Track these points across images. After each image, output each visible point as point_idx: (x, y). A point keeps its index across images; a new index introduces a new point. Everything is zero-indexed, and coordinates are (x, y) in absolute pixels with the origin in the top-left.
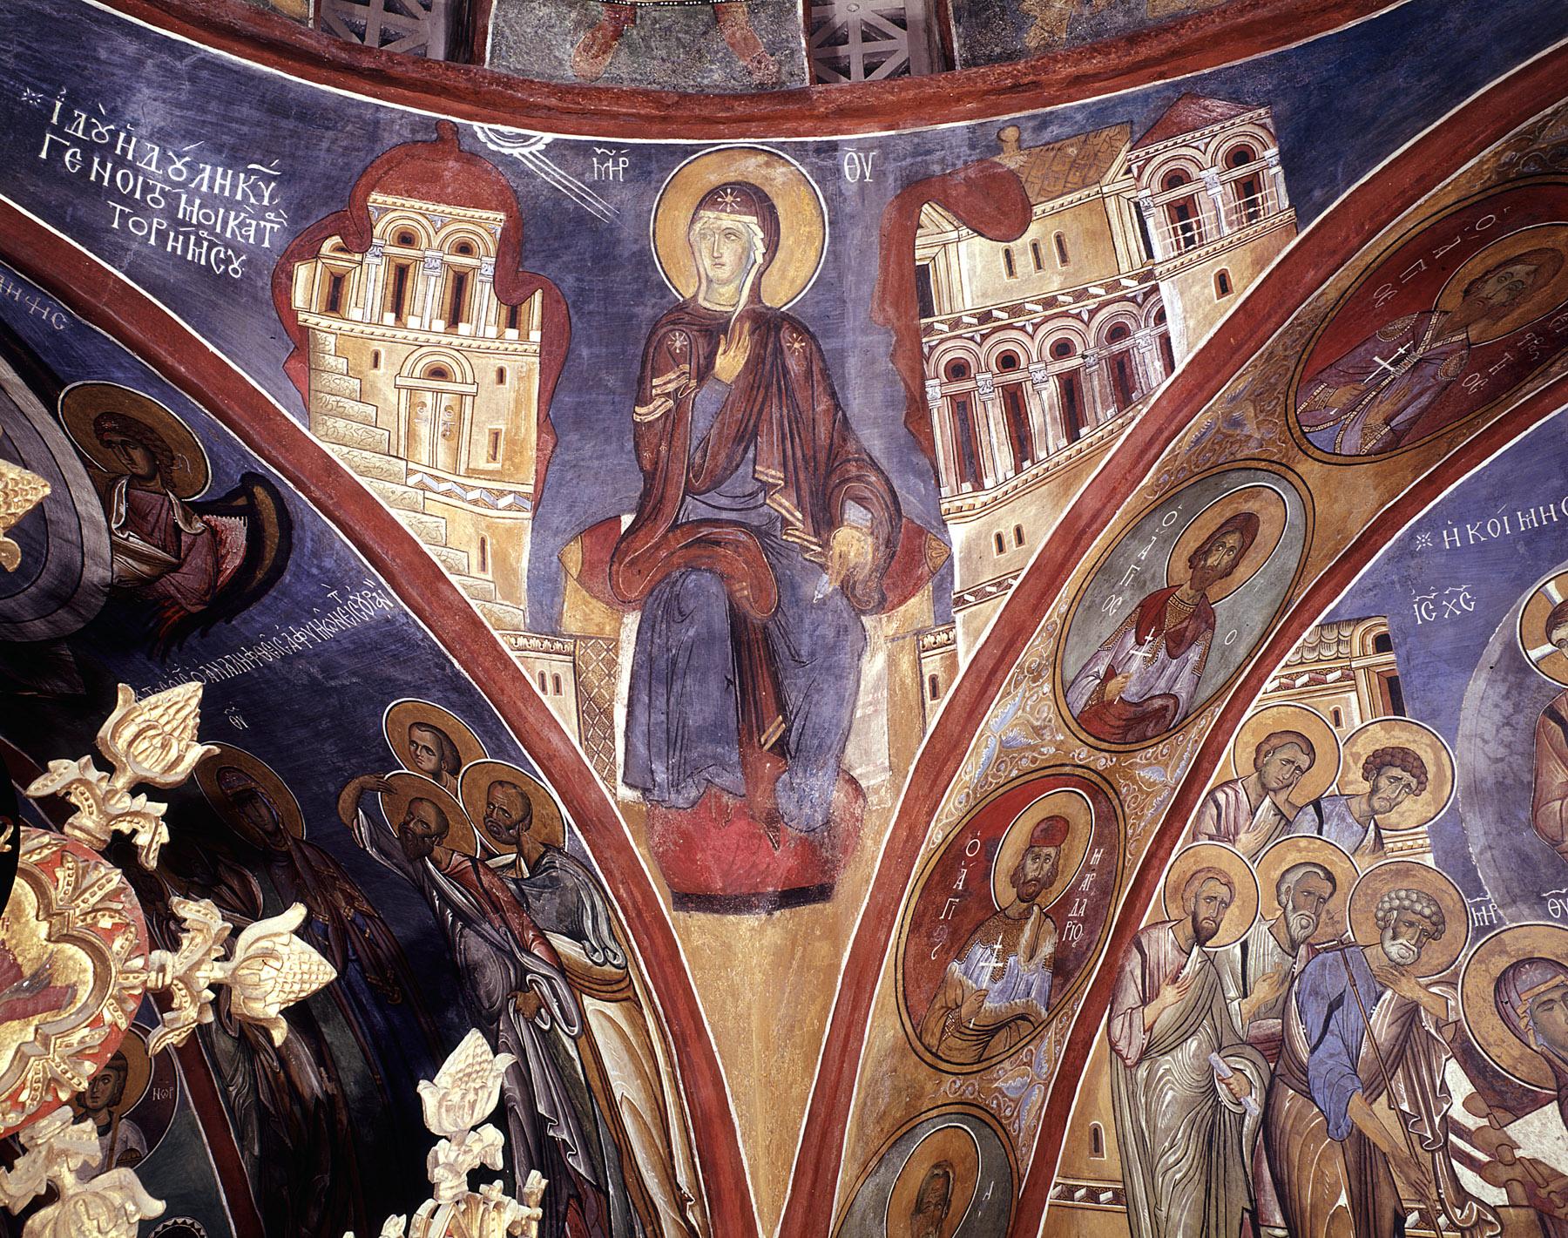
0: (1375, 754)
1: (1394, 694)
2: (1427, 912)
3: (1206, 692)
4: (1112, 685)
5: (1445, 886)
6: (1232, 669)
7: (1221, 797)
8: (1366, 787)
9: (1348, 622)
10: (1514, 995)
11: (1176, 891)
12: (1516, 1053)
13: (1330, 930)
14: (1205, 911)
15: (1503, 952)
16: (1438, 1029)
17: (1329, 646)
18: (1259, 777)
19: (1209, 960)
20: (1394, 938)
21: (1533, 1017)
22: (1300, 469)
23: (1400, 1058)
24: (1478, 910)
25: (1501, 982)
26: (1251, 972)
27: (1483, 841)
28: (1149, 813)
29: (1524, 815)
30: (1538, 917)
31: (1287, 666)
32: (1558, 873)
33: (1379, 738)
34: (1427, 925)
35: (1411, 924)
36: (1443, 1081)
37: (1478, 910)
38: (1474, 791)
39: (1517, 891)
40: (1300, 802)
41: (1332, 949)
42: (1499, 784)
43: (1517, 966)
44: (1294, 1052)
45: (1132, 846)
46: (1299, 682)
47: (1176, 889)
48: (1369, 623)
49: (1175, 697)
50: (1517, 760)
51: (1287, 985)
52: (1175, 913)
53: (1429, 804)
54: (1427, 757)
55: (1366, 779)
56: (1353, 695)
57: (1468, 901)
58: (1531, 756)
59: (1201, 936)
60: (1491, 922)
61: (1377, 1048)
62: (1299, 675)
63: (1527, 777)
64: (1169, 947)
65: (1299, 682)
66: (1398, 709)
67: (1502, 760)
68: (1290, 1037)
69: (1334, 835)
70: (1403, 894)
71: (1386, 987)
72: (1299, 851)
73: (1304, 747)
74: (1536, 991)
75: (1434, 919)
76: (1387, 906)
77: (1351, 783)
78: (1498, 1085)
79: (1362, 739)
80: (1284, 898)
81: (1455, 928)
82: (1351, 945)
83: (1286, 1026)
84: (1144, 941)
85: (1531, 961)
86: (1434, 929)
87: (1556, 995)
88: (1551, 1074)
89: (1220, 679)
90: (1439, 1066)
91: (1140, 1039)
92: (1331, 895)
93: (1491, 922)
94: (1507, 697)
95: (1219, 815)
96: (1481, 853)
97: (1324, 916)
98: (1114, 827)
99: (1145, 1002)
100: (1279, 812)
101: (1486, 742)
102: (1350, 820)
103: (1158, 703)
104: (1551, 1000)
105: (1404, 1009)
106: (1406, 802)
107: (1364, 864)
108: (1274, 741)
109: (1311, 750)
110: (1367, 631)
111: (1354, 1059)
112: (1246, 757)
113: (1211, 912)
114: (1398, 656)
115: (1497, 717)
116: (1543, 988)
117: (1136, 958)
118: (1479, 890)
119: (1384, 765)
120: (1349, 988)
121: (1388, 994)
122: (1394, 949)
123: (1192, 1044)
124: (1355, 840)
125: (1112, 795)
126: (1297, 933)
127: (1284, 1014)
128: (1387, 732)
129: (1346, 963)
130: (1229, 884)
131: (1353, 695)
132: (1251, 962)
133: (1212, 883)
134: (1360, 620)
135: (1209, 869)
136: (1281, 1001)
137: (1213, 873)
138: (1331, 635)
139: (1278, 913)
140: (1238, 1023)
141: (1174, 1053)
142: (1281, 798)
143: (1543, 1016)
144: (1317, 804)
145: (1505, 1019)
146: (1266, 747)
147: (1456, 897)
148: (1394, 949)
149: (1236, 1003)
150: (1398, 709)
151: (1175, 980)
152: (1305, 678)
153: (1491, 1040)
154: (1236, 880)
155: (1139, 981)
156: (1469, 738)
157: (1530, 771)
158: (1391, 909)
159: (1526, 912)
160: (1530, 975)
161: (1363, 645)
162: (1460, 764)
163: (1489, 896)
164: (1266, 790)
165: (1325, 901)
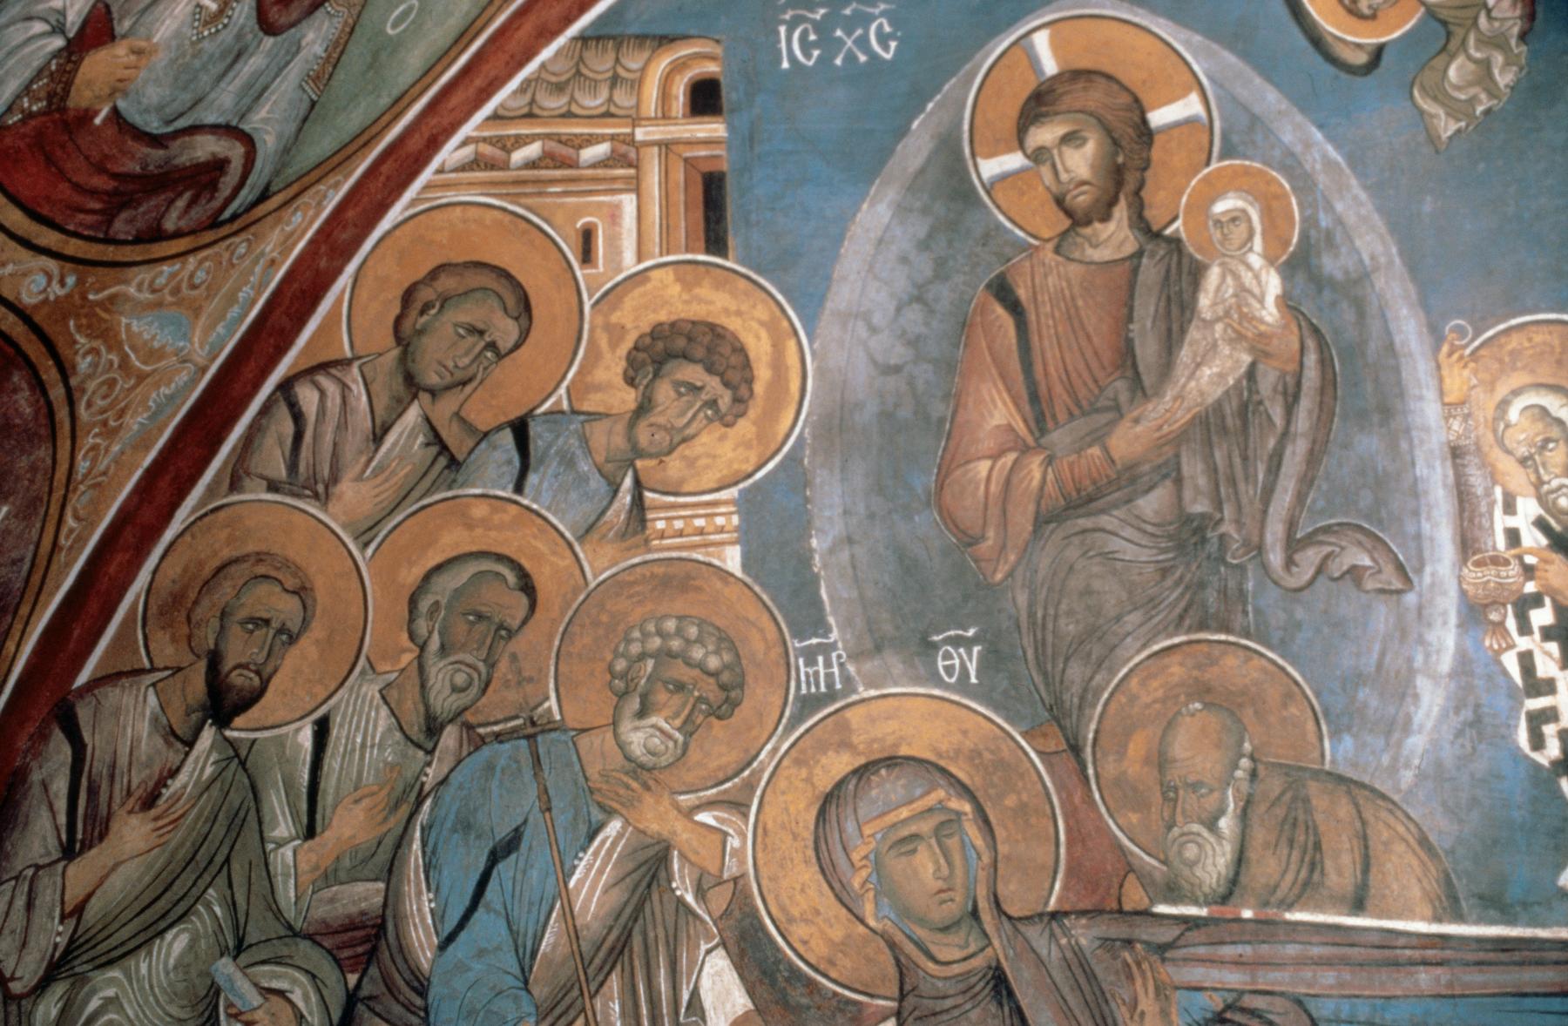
0: (657, 332)
1: (712, 207)
2: (713, 663)
3: (321, 144)
4: (98, 66)
5: (753, 612)
6: (385, 101)
7: (307, 397)
8: (628, 398)
9: (641, 39)
10: (850, 826)
11: (173, 607)
12: (837, 934)
13: (513, 696)
14: (240, 650)
15: (846, 745)
16: (700, 893)
17: (594, 86)
18: (404, 359)
19: (238, 757)
20: (642, 713)
21: (878, 866)
23: (620, 950)
24: (811, 662)
25: (830, 802)
26: (329, 784)
27: (838, 529)
28: (135, 422)
29: (923, 481)
30: (917, 681)
31: (495, 117)
32: (966, 598)
33: (671, 300)
34: (710, 689)
35: (680, 687)
36: (695, 994)
37: (811, 662)
38: (835, 428)
39: (888, 628)
40: (483, 421)
41: (512, 734)
42: (886, 416)
43: (862, 772)
44: (402, 950)
45: (80, 500)
46: (518, 156)
47: (177, 598)
48: (684, 50)
49: (248, 140)
50: (924, 373)
51: (405, 810)
52: (167, 651)
53: (748, 445)
54: (759, 347)
55: (631, 381)
56: (628, 202)
57: (795, 644)
58: (948, 367)
59: (223, 704)
60: (830, 685)
61: (575, 934)
62: (520, 141)
63: (938, 409)
64: (145, 728)
65: (518, 156)
66: (715, 241)
67: (897, 369)
68: (399, 918)
69: (546, 497)
70: (671, 625)
71: (610, 813)
72: (470, 526)
73: (511, 301)
74: (891, 818)
75: (726, 677)
76: (635, 649)
77: (598, 388)
78: (798, 996)
79: (631, 300)
80: (422, 626)
81: (760, 696)
82: (551, 727)
83: (392, 899)
84: (84, 713)
85: (892, 761)
86: (726, 697)
87: (925, 827)
88: (892, 971)
89: (354, 120)
90: (692, 962)
91: (52, 934)
92: (524, 622)
93: (830, 685)
94: (924, 245)
95: (298, 437)
96: (832, 551)
97: (503, 666)
98: (43, 452)
99: (70, 851)
100: (436, 439)
101: (873, 330)
102: (584, 466)
103: (206, 147)
104: (915, 837)
105: (642, 856)
106: (704, 438)
107: (600, 564)
108: (447, 283)
109: (524, 308)
110: (678, 67)
111: (526, 957)
112: (382, 308)
113: (255, 653)
114: (731, 128)
115: (901, 284)
116: (904, 813)
117: (60, 751)
118: (821, 627)
119: (670, 355)
120: (536, 817)
121: (614, 827)
122: (638, 738)
123: (176, 943)
124: (588, 510)
125: (50, 374)
126: (443, 700)
127: (391, 871)
128: (687, 286)
129: (537, 761)
130: (302, 592)
131: (628, 202)
132: (332, 763)
133: (263, 589)
134: (665, 40)
135: (260, 557)
136: (389, 842)
137: (264, 566)
138: (600, 63)
139: (407, 658)
140: (287, 893)
141: (131, 962)
142: (443, 410)
143: (897, 865)
144: (520, 430)
145: (827, 870)
146: (425, 294)
147: (771, 633)
148: (638, 738)
149: (287, 852)
150: (715, 241)
151: (150, 801)
152: (533, 150)
153: (795, 912)
154: (320, 585)
155: (61, 805)
156: (845, 318)
157: (946, 397)
158: (642, 657)
159: (897, 667)
160: (888, 788)
161: (665, 96)
162: (820, 372)
163: (834, 635)
164: (412, 385)
165: (511, 634)
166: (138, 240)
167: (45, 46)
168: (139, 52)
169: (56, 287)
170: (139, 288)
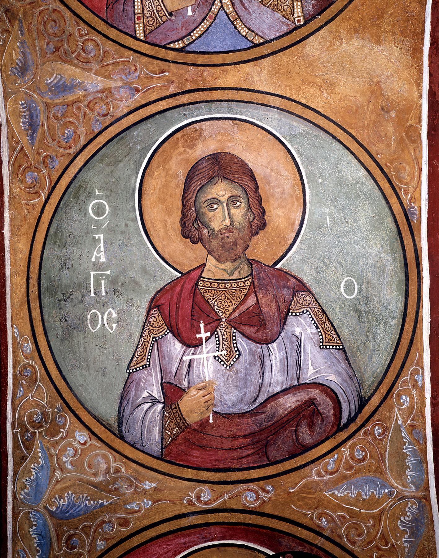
6: (395, 323)
22: (222, 82)
103: (290, 402)
166: (292, 456)
167: (154, 412)
168: (204, 388)
169: (262, 495)
170: (319, 474)
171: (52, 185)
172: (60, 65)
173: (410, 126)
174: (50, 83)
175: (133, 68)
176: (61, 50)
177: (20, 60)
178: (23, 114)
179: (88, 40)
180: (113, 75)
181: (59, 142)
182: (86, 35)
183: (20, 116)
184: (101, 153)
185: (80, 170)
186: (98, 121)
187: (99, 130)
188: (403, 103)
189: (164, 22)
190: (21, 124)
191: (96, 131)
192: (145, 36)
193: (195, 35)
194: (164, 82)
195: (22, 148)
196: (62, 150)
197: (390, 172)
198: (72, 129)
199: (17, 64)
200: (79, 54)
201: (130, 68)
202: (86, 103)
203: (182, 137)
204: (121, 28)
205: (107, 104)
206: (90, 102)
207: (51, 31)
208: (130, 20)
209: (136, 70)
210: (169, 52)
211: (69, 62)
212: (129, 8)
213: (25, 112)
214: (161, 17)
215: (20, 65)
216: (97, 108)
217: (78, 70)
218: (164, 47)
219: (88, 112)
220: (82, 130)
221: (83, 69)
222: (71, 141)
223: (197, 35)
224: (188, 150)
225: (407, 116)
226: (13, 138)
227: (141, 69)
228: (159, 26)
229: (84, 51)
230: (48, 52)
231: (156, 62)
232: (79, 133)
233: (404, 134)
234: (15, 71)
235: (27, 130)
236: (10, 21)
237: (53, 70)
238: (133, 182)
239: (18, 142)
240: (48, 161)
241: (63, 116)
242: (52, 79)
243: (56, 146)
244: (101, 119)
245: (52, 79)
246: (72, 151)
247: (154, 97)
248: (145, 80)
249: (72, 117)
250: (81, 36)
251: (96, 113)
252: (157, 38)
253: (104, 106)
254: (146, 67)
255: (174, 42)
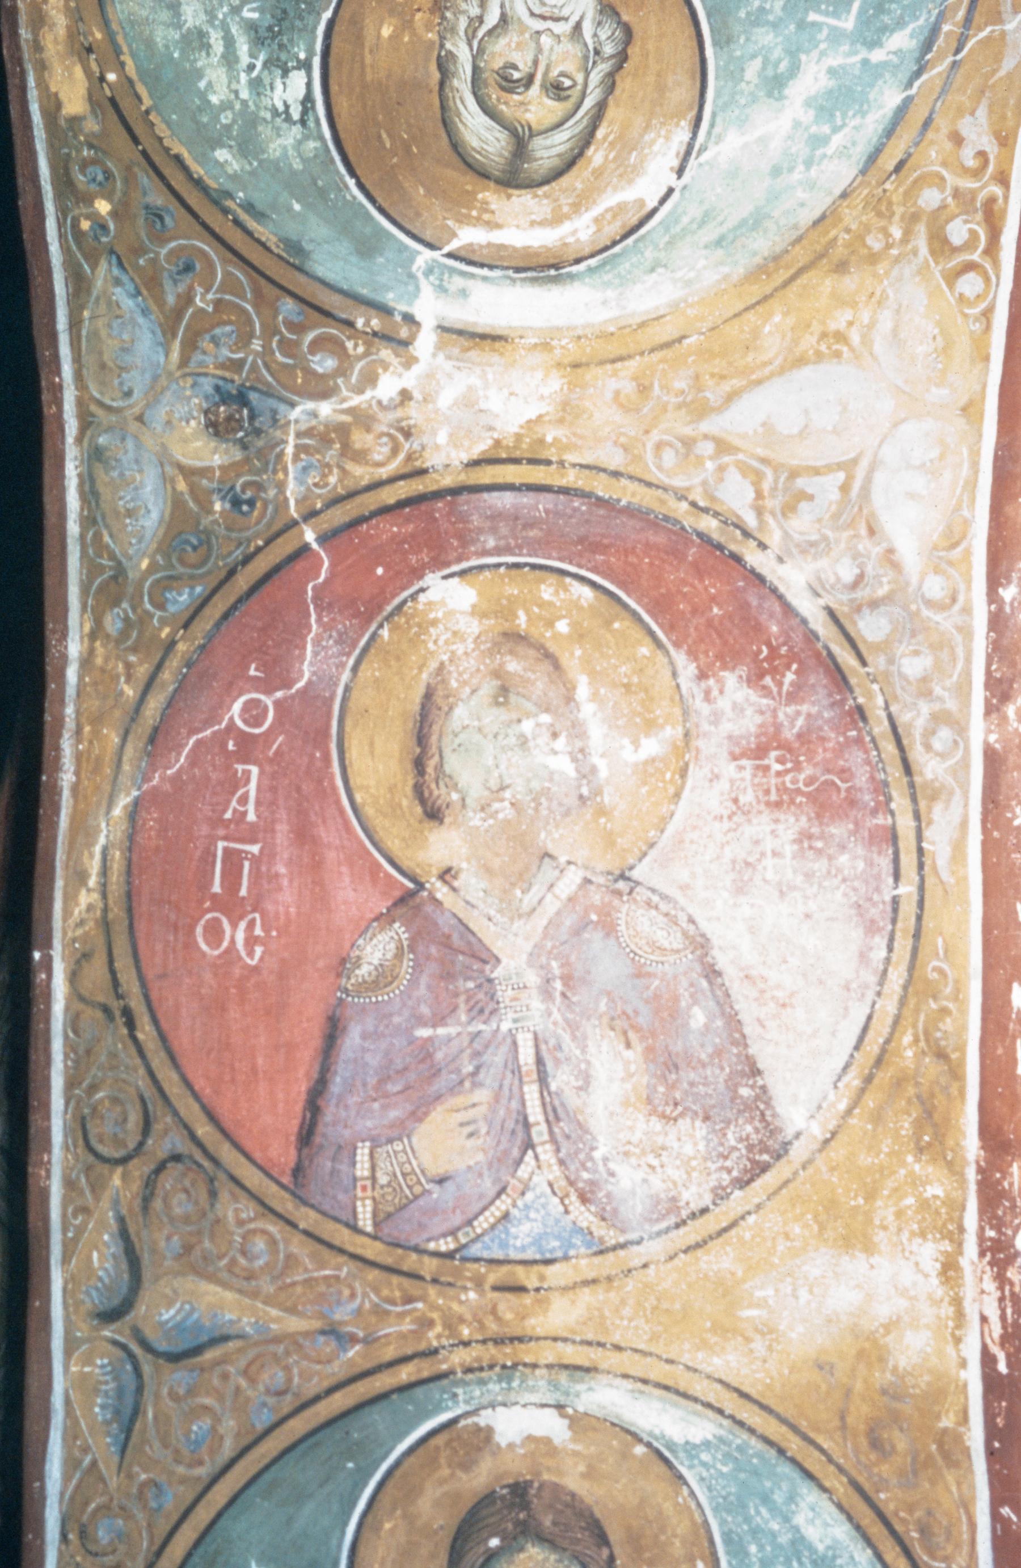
171: (155, 1548)
172: (190, 1283)
173: (945, 1431)
174: (167, 1322)
175: (346, 1292)
176: (197, 1252)
177: (106, 1270)
178: (104, 1387)
179: (254, 1232)
180: (304, 1305)
181: (177, 1451)
182: (251, 1220)
183: (96, 1391)
184: (267, 1477)
185: (219, 1515)
186: (264, 1404)
187: (267, 1424)
188: (926, 1378)
189: (416, 1197)
190: (97, 1410)
191: (260, 1427)
192: (376, 1224)
193: (482, 1224)
194: (412, 1322)
195: (94, 1463)
196: (181, 1470)
197: (908, 1531)
198: (206, 1423)
199: (100, 1279)
200: (233, 1262)
201: (340, 1293)
202: (243, 1363)
203: (448, 1443)
204: (326, 1207)
205: (287, 1369)
206: (249, 1365)
207: (178, 1211)
208: (346, 1191)
209: (353, 1296)
210: (426, 1259)
211: (212, 1278)
212: (344, 1167)
213: (106, 1383)
214: (410, 1187)
215: (107, 1280)
216: (265, 1376)
217: (229, 1295)
218: (417, 1250)
219: (243, 1383)
220: (229, 1425)
221: (240, 1291)
222: (204, 1449)
223: (485, 1225)
224: (459, 1473)
225: (936, 1408)
226: (75, 1438)
227: (365, 1295)
228: (406, 1206)
229: (244, 1253)
230: (168, 1255)
231: (395, 1279)
232: (221, 1430)
233: (934, 1447)
234: (94, 1293)
235: (107, 1423)
236: (93, 1190)
237: (175, 1292)
238: (334, 1542)
239: (86, 1449)
240: (150, 1493)
241: (191, 1392)
242: (172, 1312)
243: (170, 1460)
244: (271, 1401)
245: (172, 1312)
246: (203, 1472)
247: (390, 1353)
248: (373, 1319)
249: (208, 1394)
250: (241, 1223)
251: (261, 1387)
252: (402, 1229)
253: (281, 1374)
254: (377, 1291)
255: (436, 1239)
